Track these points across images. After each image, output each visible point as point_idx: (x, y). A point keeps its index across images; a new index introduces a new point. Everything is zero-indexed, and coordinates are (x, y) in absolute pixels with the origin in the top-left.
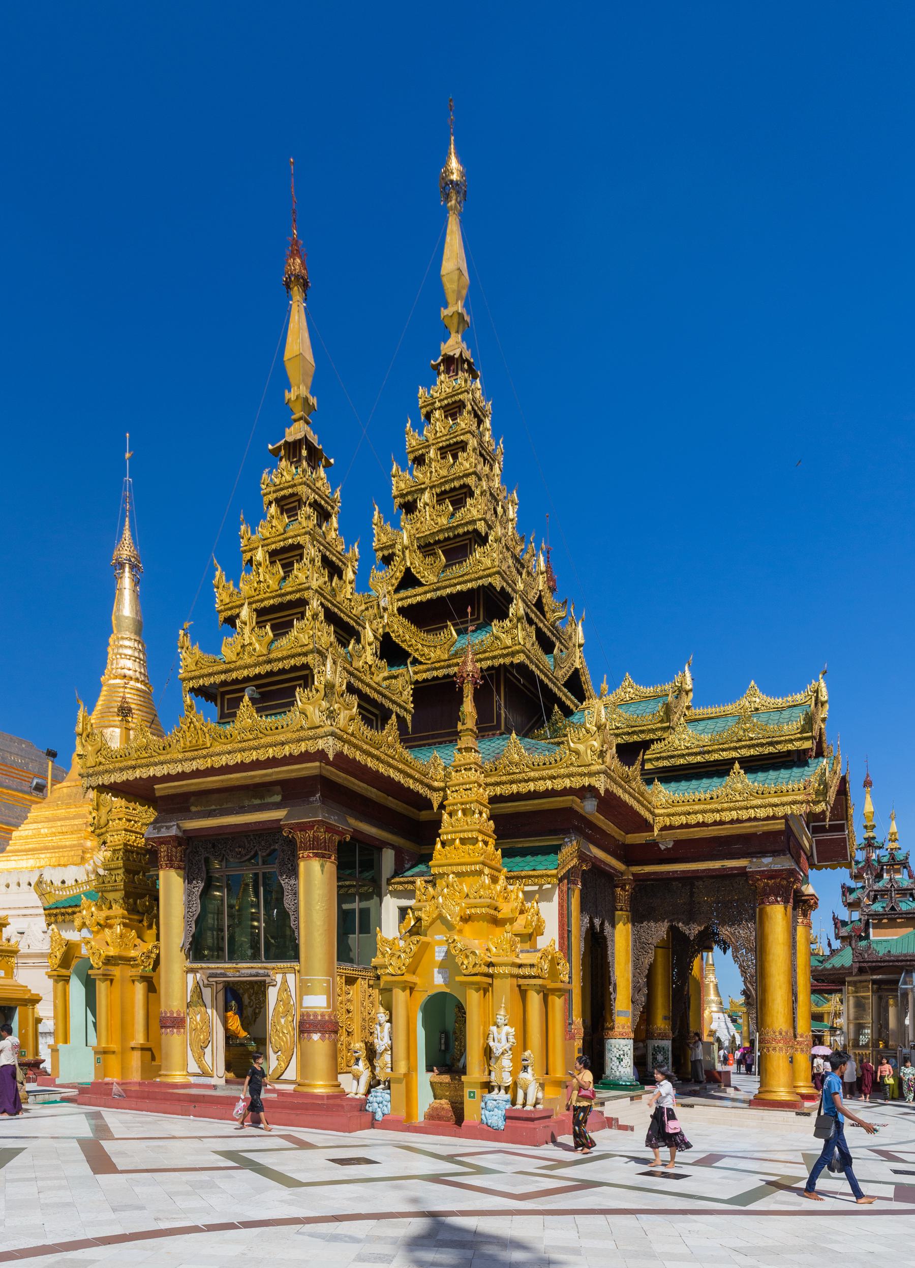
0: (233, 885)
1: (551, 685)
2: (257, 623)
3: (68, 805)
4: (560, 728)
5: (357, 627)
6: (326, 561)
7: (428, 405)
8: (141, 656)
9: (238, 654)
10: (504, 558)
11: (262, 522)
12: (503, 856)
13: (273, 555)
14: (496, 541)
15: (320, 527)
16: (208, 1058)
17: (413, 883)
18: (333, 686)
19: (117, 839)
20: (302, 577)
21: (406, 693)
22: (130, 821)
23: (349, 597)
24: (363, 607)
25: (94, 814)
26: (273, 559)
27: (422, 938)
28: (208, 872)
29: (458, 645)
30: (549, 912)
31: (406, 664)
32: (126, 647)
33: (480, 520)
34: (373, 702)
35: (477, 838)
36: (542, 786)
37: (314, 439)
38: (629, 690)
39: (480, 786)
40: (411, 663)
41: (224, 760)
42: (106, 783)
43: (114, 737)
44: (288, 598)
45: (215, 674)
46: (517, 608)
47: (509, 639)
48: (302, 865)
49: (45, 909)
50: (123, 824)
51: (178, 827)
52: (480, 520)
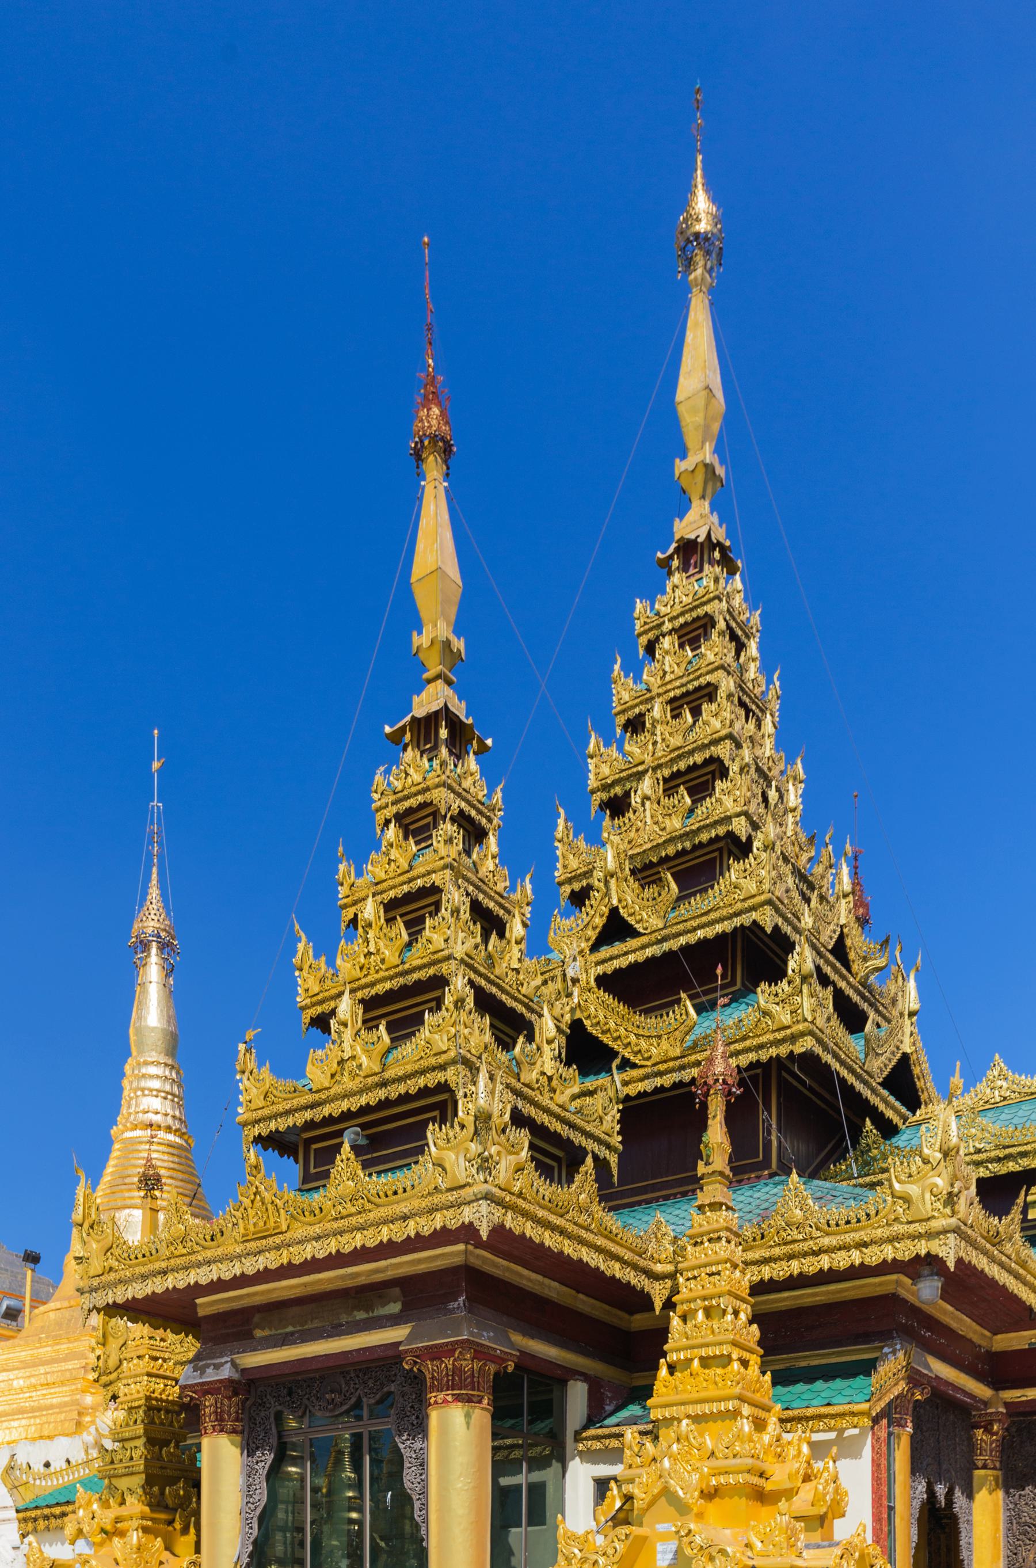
0: (322, 1455)
1: (859, 1086)
2: (364, 1022)
3: (57, 1340)
4: (874, 1159)
5: (528, 1015)
6: (478, 910)
7: (651, 629)
8: (176, 1090)
9: (333, 1076)
10: (780, 877)
11: (373, 855)
12: (774, 1384)
13: (391, 907)
14: (766, 848)
15: (468, 853)
17: (620, 1436)
18: (489, 1117)
19: (134, 1390)
20: (438, 940)
21: (609, 1118)
22: (156, 1359)
23: (515, 965)
24: (539, 981)
25: (98, 1352)
26: (391, 915)
27: (635, 1530)
28: (280, 1436)
29: (698, 1031)
30: (856, 1476)
31: (609, 1070)
32: (152, 1077)
33: (738, 815)
34: (555, 1138)
35: (729, 1356)
36: (842, 1261)
37: (459, 709)
38: (999, 1083)
39: (735, 1266)
40: (619, 1068)
41: (309, 1251)
42: (120, 1300)
43: (132, 1225)
44: (416, 976)
45: (296, 1110)
46: (802, 960)
47: (787, 1013)
48: (434, 1417)
49: (18, 1511)
50: (145, 1365)
51: (234, 1364)
52: (738, 815)
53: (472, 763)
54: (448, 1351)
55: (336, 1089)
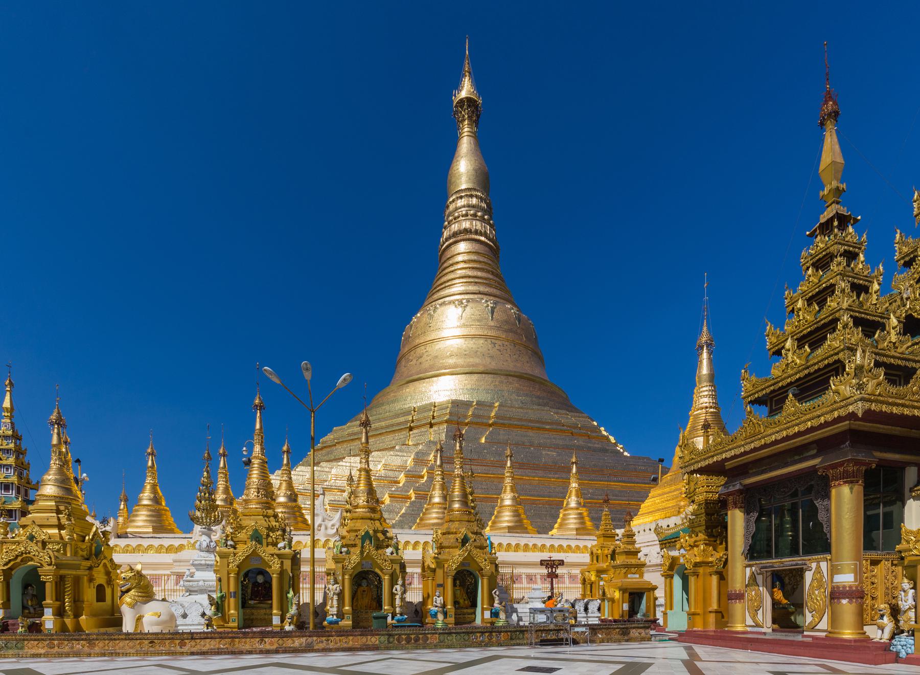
13: (810, 301)
15: (848, 265)
16: (760, 616)
19: (700, 498)
37: (843, 211)
48: (833, 491)
50: (705, 488)
51: (741, 484)
53: (851, 229)
54: (841, 464)
55: (786, 375)
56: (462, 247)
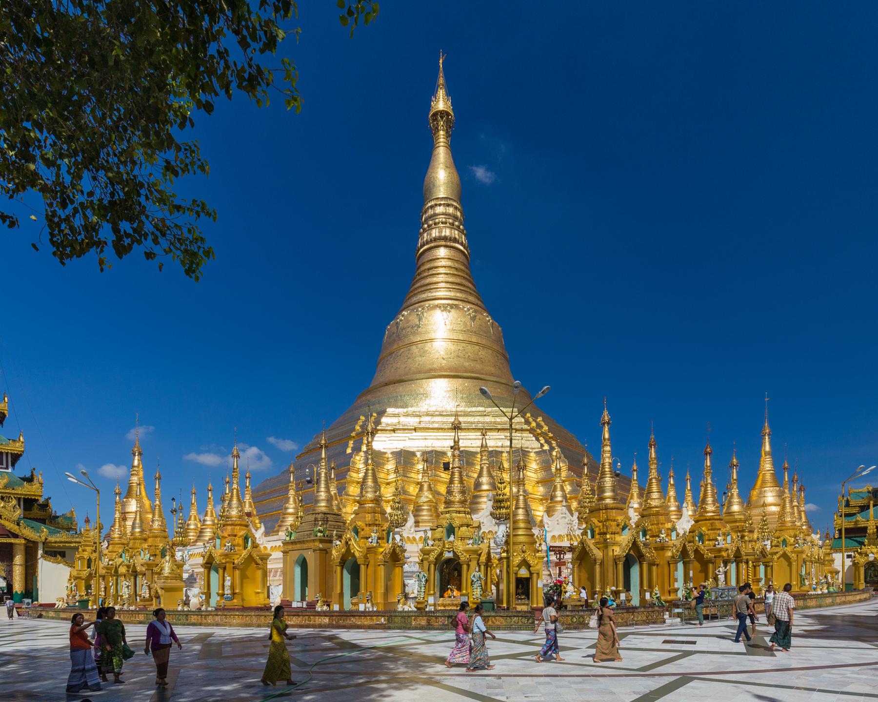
56: (442, 252)
